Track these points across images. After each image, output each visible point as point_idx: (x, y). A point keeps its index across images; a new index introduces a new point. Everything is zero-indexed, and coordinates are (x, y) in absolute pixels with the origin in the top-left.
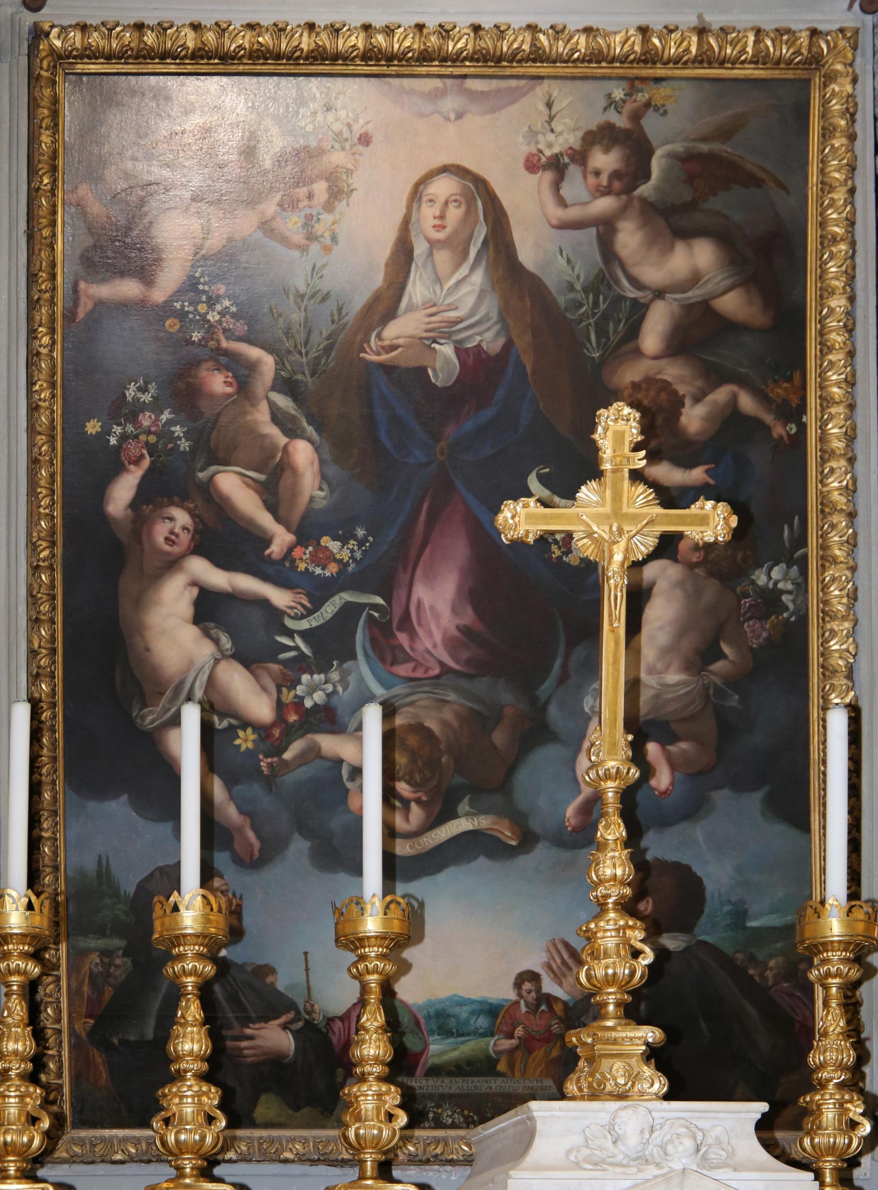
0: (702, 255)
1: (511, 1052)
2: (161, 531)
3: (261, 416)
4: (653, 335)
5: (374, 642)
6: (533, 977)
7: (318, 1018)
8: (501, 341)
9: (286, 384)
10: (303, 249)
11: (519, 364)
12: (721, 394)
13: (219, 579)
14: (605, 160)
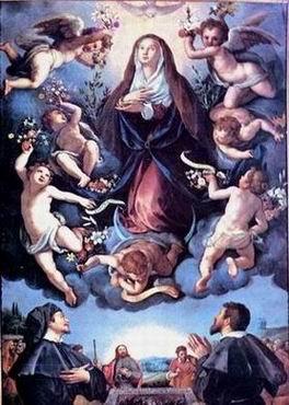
0: (248, 69)
1: (175, 378)
2: (37, 176)
3: (76, 132)
4: (230, 98)
5: (121, 219)
6: (184, 349)
7: (99, 366)
8: (170, 102)
9: (86, 118)
10: (93, 67)
11: (177, 111)
12: (256, 122)
14: (211, 33)
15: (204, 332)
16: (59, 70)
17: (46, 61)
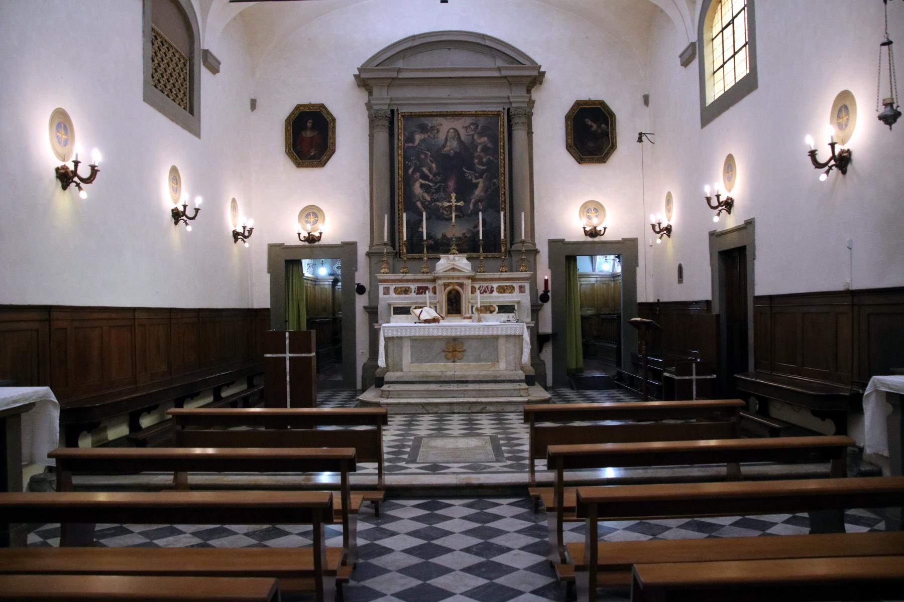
0: (485, 139)
4: (479, 150)
13: (423, 182)
15: (472, 229)
16: (423, 141)
17: (418, 137)
